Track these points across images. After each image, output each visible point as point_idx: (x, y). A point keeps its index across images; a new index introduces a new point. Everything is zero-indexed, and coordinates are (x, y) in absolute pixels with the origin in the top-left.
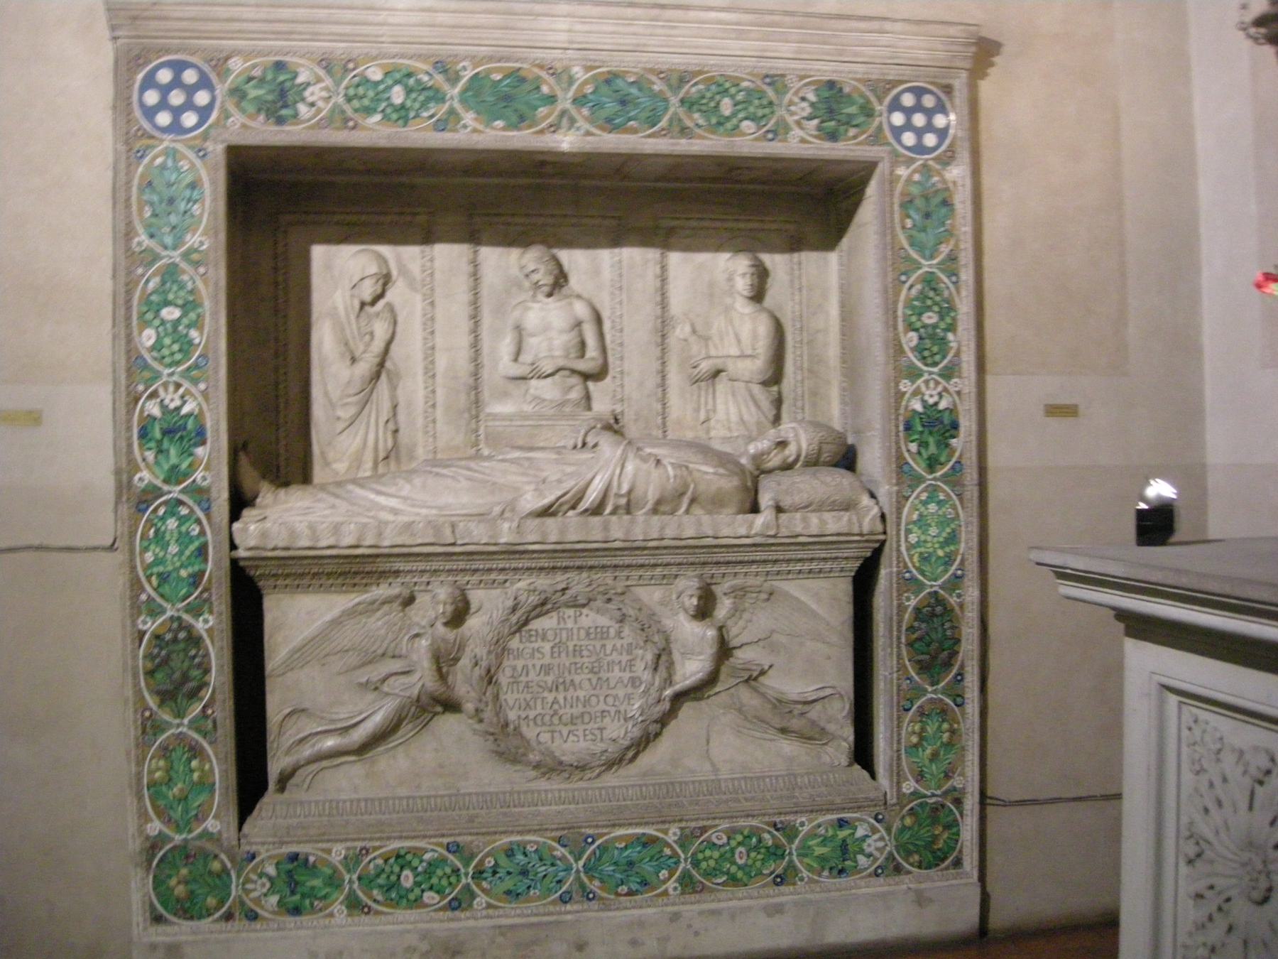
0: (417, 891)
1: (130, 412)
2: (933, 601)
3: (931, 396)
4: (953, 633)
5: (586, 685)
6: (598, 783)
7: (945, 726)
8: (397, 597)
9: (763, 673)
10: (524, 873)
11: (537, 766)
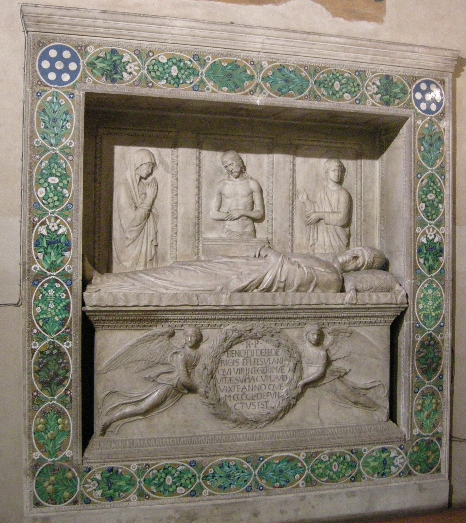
0: (174, 487)
1: (31, 232)
2: (429, 338)
3: (431, 235)
4: (438, 355)
5: (260, 379)
6: (265, 430)
7: (434, 401)
8: (167, 332)
9: (346, 374)
10: (228, 476)
11: (235, 421)
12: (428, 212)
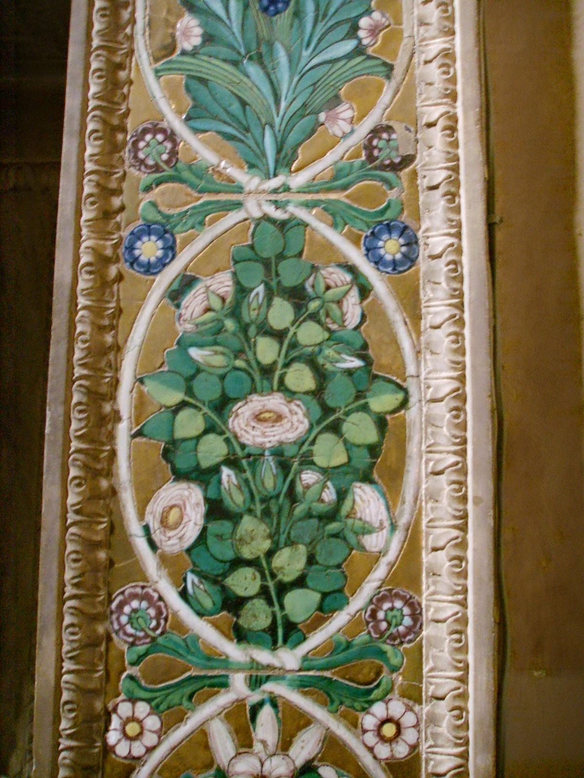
12: (238, 563)
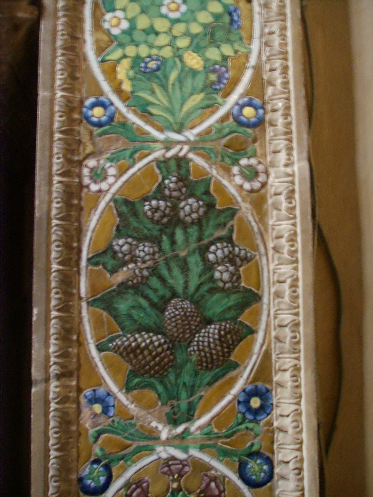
2: (171, 183)
4: (236, 277)
